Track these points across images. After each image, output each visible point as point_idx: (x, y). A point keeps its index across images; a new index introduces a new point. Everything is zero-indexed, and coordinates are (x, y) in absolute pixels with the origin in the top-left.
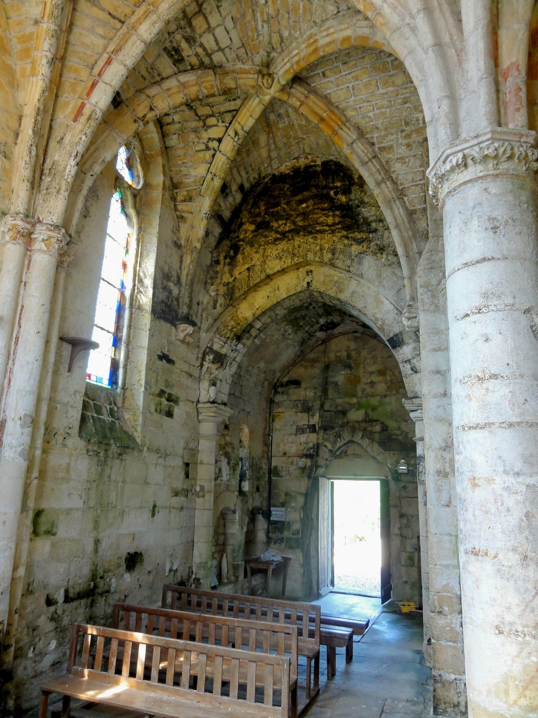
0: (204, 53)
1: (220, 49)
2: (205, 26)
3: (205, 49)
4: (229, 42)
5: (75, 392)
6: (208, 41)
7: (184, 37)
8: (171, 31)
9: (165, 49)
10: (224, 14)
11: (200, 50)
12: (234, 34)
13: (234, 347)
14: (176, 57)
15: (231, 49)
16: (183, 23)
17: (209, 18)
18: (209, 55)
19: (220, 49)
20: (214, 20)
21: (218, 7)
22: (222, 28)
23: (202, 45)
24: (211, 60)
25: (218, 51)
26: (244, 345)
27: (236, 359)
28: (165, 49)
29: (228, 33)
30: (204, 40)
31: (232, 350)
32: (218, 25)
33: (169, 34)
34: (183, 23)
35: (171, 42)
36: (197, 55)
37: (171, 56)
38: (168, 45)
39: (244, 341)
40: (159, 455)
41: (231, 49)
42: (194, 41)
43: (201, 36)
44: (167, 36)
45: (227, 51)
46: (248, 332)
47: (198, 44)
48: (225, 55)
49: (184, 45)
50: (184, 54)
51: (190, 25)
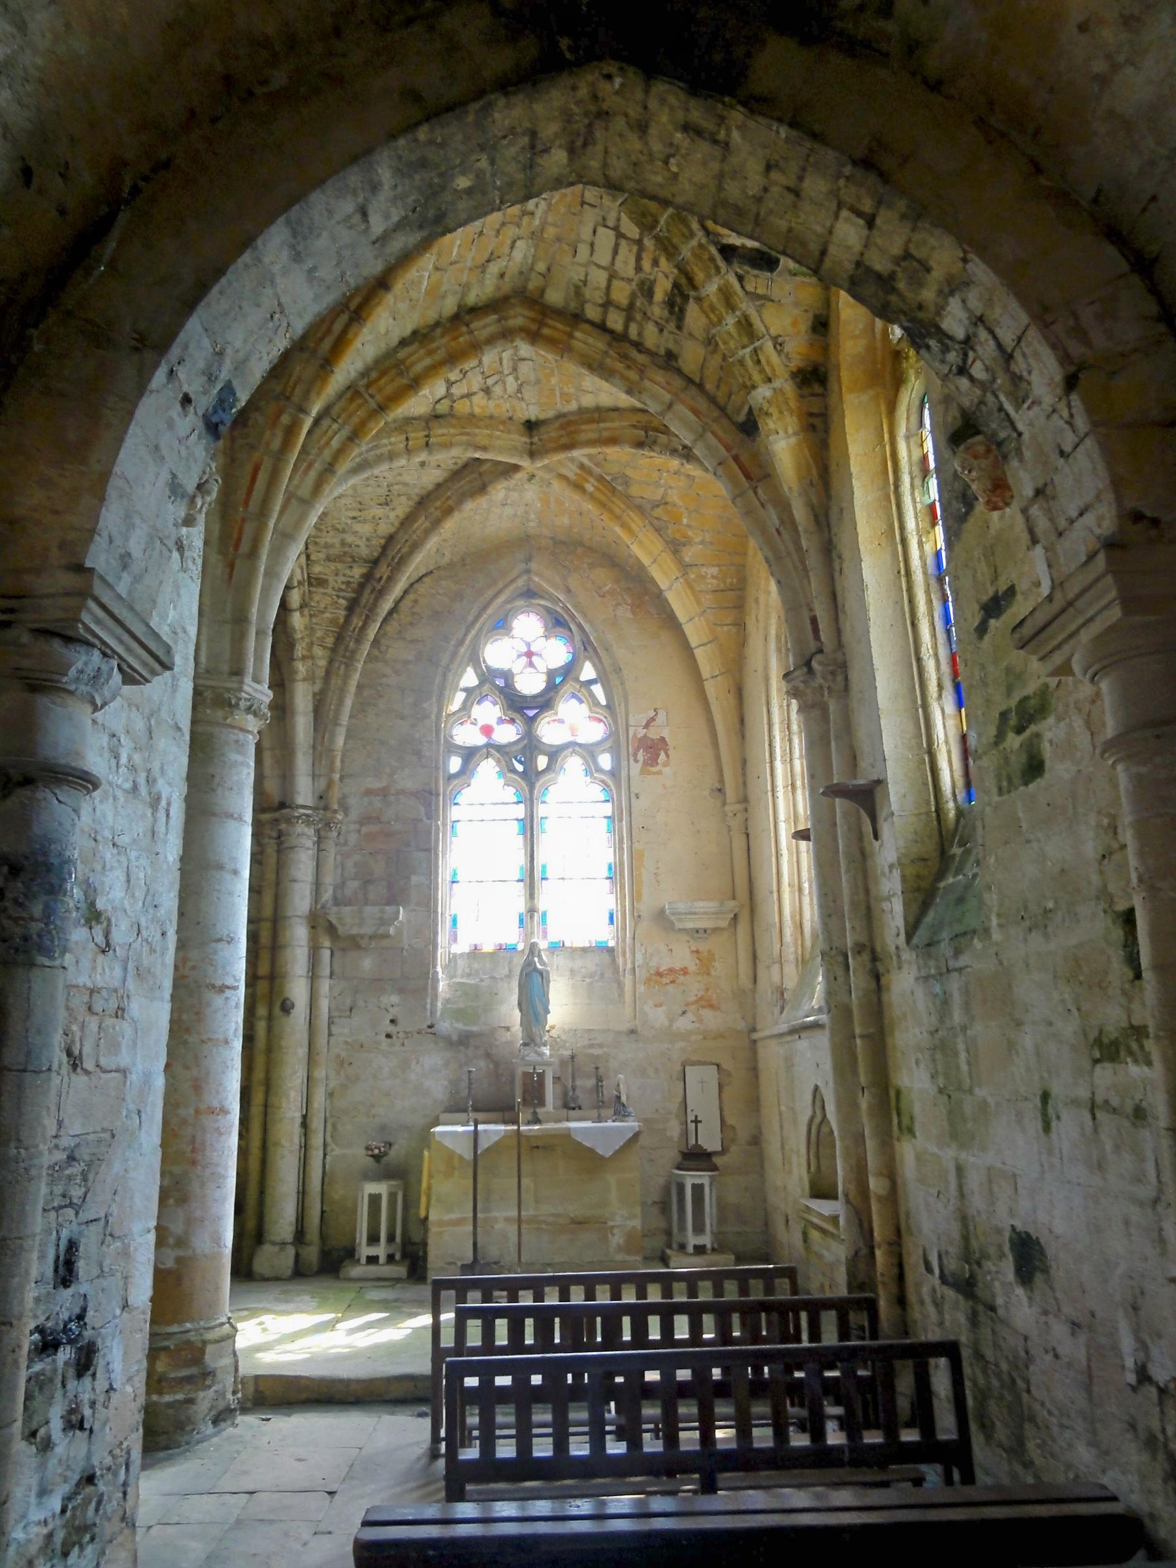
0: (644, 255)
1: (620, 235)
2: (616, 283)
3: (639, 259)
4: (601, 230)
5: (891, 866)
6: (626, 262)
7: (651, 302)
8: (656, 330)
9: (679, 328)
10: (582, 270)
11: (646, 264)
12: (586, 233)
13: (953, 357)
14: (678, 300)
15: (604, 219)
16: (638, 316)
17: (603, 285)
18: (639, 242)
19: (620, 235)
20: (599, 278)
21: (585, 282)
22: (595, 258)
23: (638, 269)
24: (641, 234)
25: (623, 236)
26: (954, 286)
27: (1007, 337)
28: (679, 328)
29: (592, 245)
30: (630, 271)
31: (962, 370)
32: (599, 266)
33: (661, 331)
34: (638, 316)
35: (667, 321)
36: (655, 263)
37: (682, 311)
38: (672, 326)
39: (928, 295)
40: (1027, 923)
41: (604, 219)
42: (642, 283)
43: (630, 280)
44: (665, 332)
45: (611, 223)
46: (886, 282)
47: (642, 276)
48: (618, 220)
49: (659, 296)
50: (668, 285)
51: (631, 305)
